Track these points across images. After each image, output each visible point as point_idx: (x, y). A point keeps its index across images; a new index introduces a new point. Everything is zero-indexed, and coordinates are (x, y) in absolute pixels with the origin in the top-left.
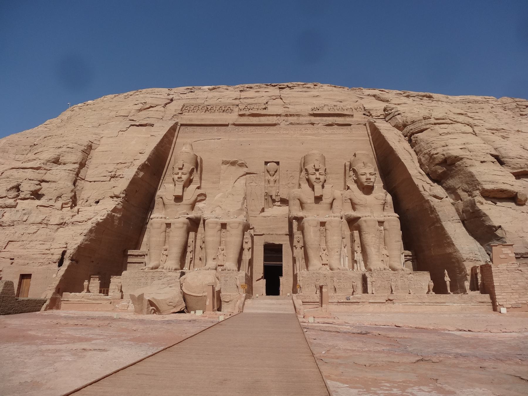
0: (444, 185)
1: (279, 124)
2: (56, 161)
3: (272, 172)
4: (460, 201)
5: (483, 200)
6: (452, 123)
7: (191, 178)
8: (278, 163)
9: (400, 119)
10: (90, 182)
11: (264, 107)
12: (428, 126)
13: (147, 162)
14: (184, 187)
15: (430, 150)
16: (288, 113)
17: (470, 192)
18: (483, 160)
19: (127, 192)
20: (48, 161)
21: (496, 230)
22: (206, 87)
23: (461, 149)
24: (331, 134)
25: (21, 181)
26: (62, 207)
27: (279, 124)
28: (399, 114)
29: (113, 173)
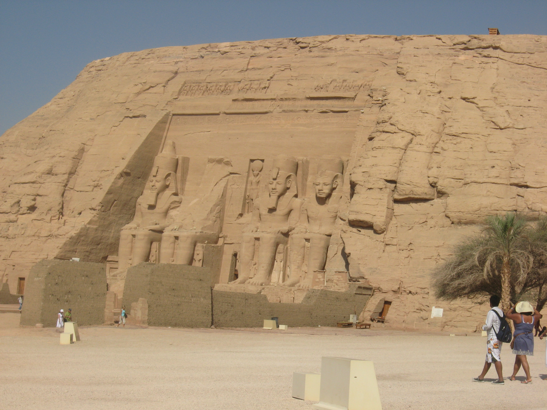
1: (271, 112)
2: (50, 173)
3: (256, 172)
5: (351, 229)
7: (167, 184)
8: (263, 161)
13: (125, 171)
14: (158, 194)
16: (284, 97)
18: (369, 187)
19: (102, 204)
20: (43, 173)
21: (348, 256)
22: (224, 46)
25: (20, 197)
26: (51, 220)
27: (271, 112)
29: (96, 182)
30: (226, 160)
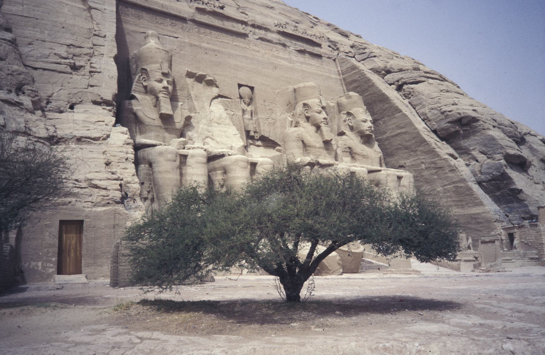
0: (453, 144)
1: (248, 36)
3: (247, 100)
4: (474, 162)
6: (442, 81)
8: (252, 88)
9: (379, 63)
10: (36, 69)
11: (221, 5)
12: (423, 79)
15: (439, 105)
17: (490, 154)
23: (474, 110)
24: (304, 63)
28: (375, 56)
29: (72, 61)
30: (208, 78)
